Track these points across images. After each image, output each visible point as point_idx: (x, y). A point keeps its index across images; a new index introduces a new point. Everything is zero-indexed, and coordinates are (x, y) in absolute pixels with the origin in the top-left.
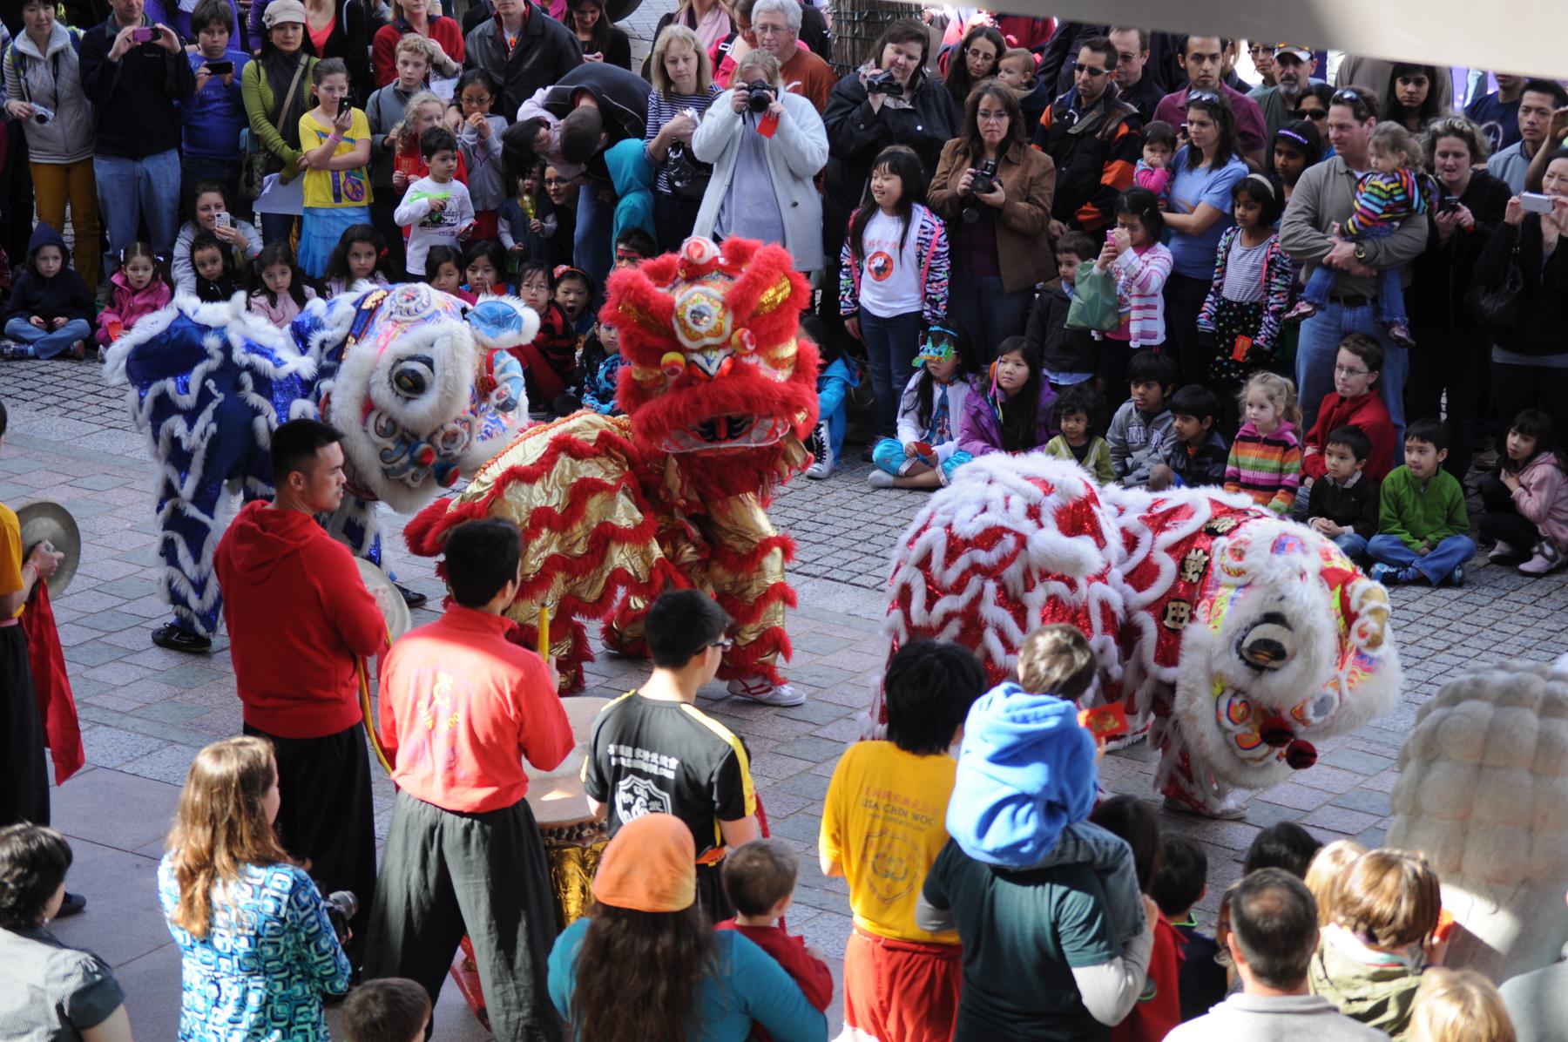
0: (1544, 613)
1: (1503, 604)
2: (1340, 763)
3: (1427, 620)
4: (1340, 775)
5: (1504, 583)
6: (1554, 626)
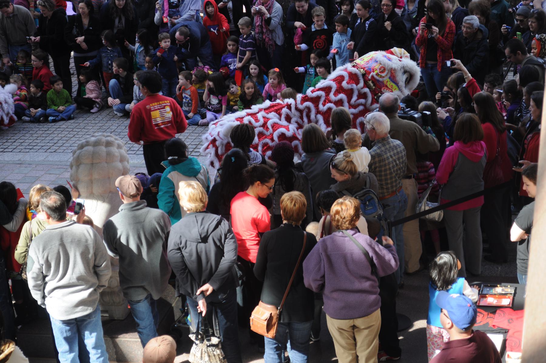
0: (97, 122)
1: (86, 122)
2: (51, 173)
3: (67, 130)
4: (52, 176)
5: (85, 116)
6: (101, 125)
